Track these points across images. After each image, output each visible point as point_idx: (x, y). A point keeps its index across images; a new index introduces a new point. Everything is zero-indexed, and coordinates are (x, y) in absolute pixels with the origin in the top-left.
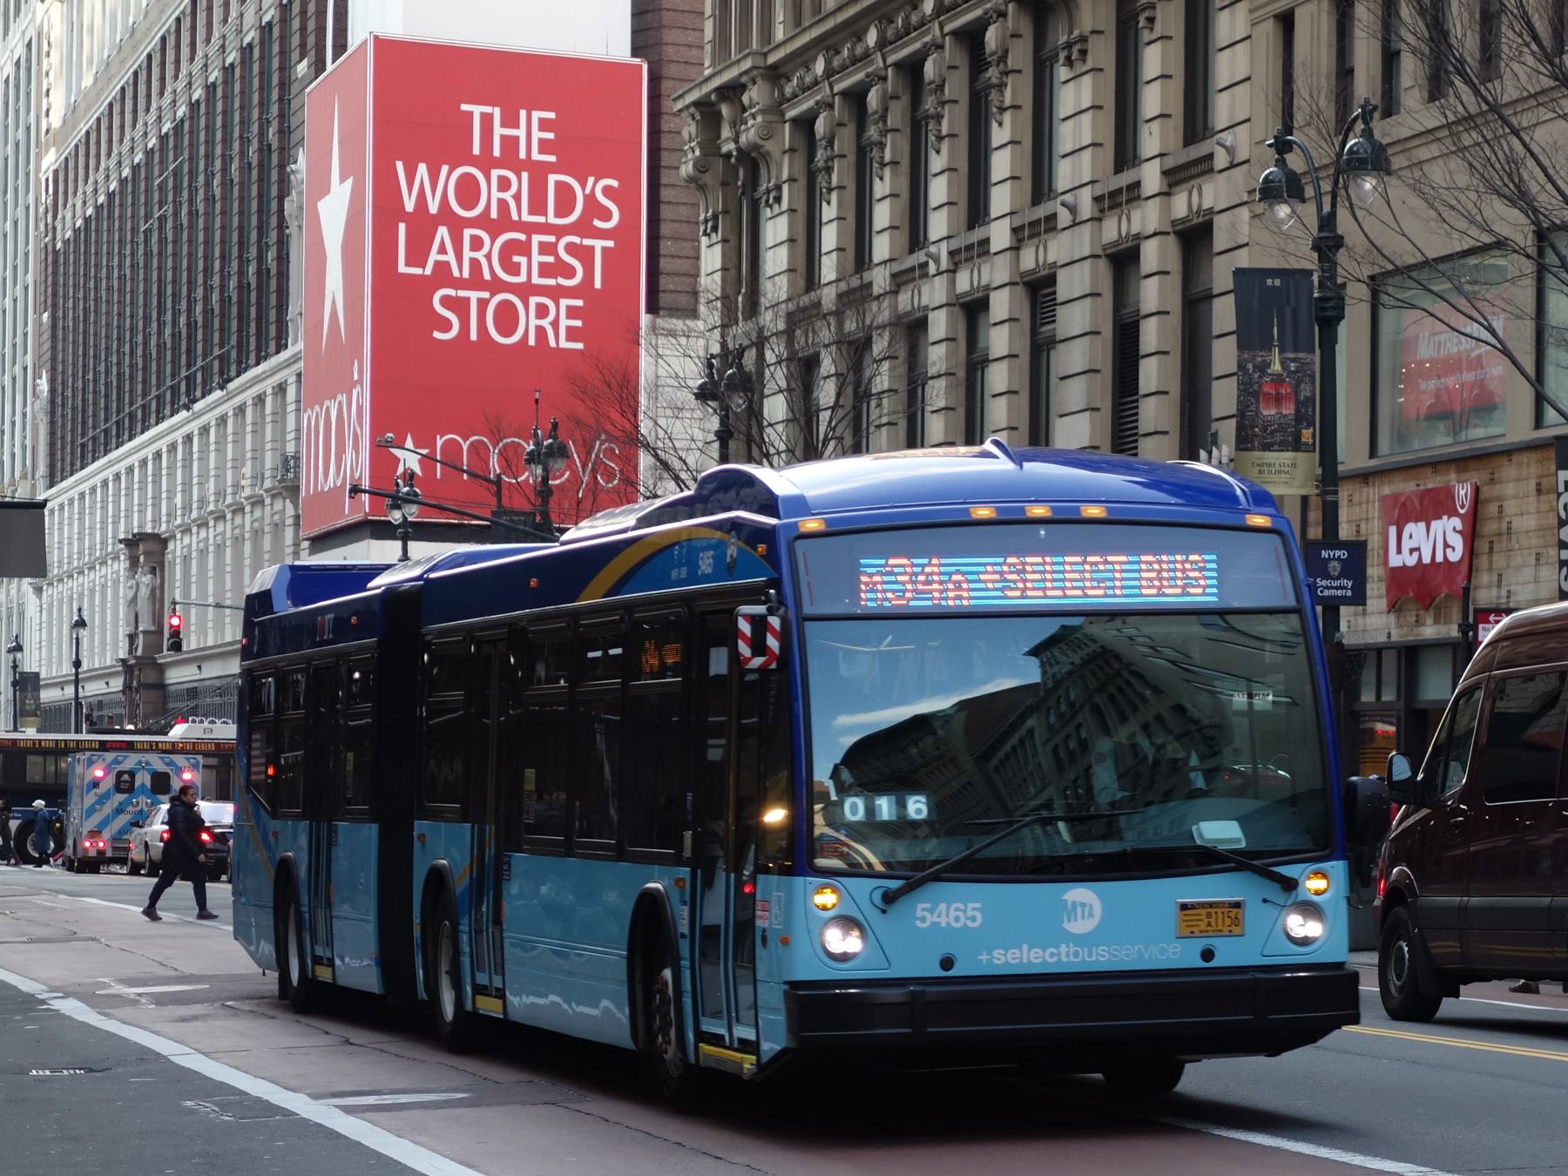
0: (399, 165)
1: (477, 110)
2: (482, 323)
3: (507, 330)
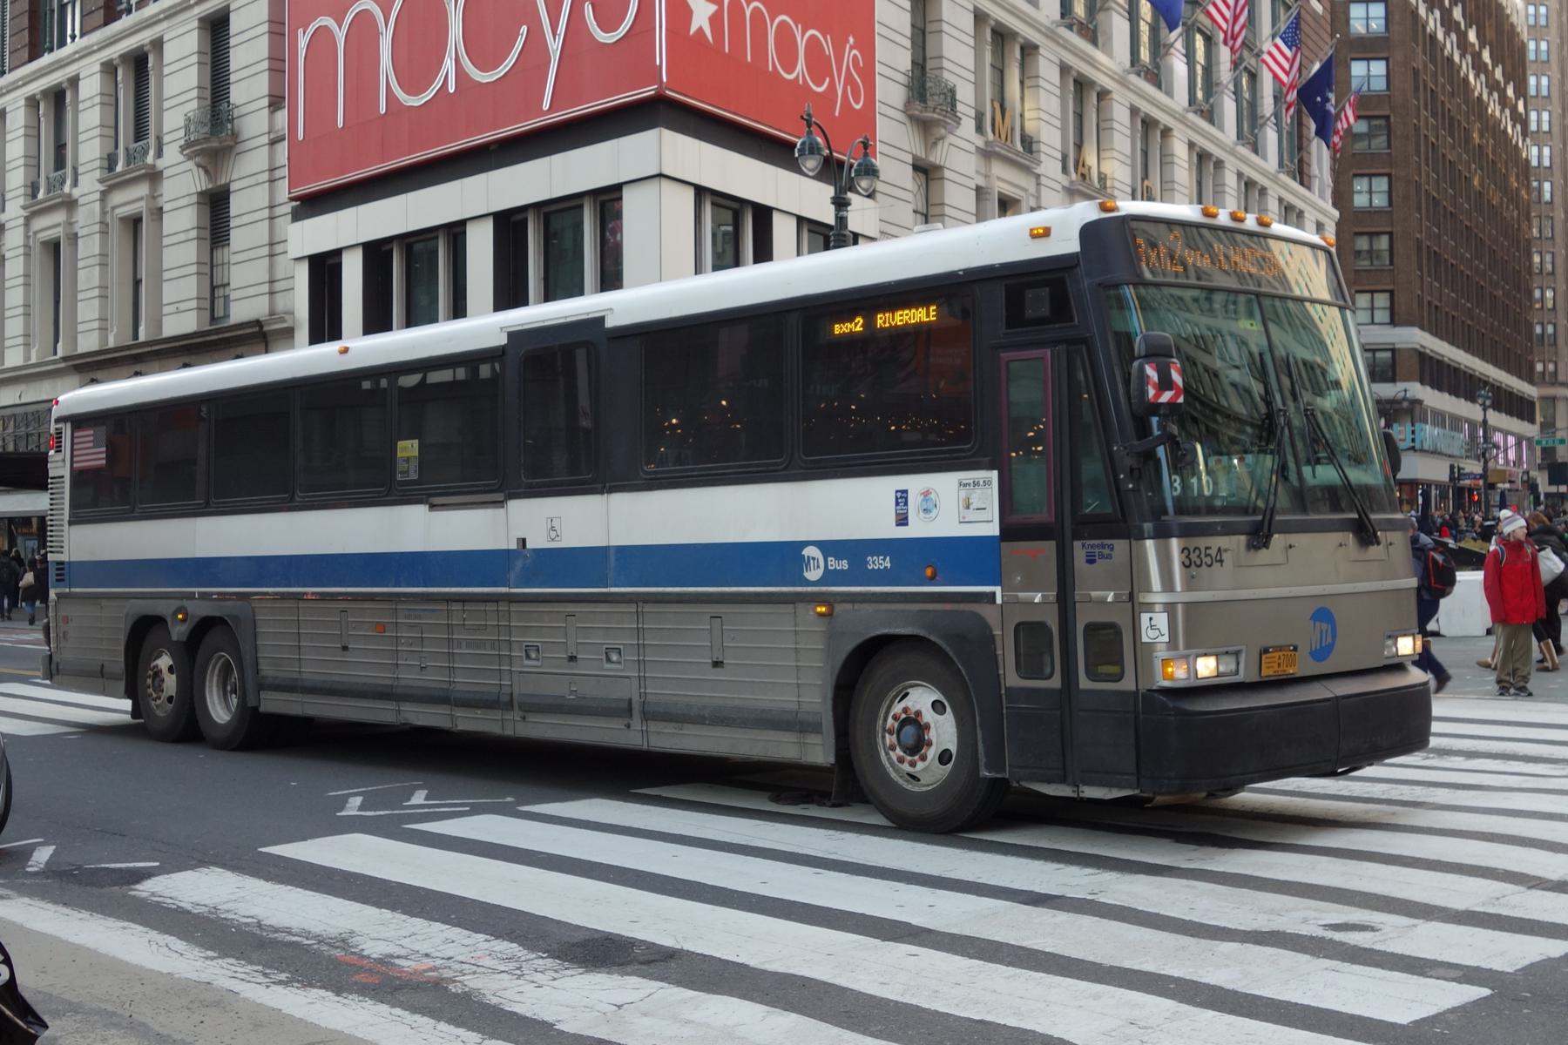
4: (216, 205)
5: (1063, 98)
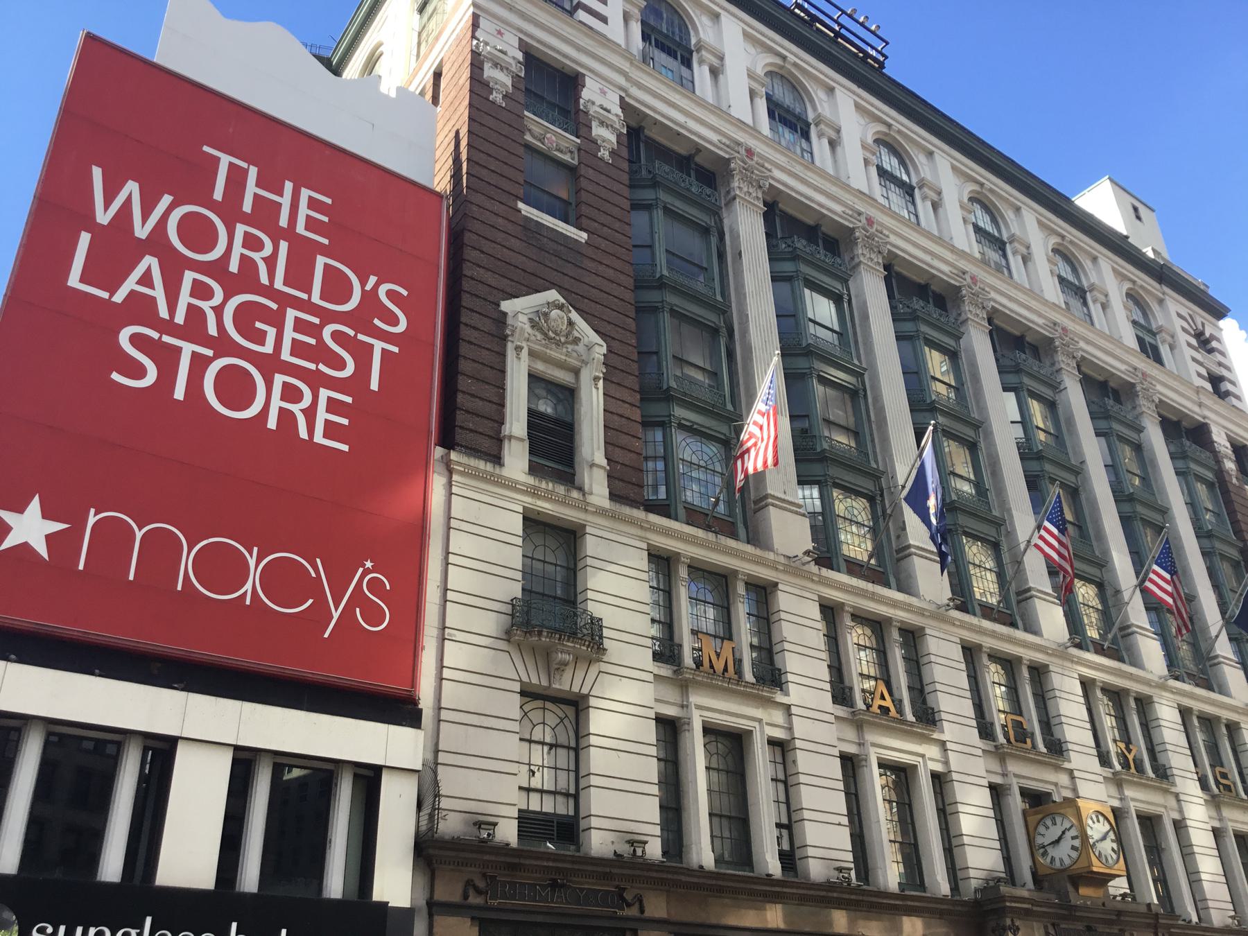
0: (97, 173)
1: (225, 160)
2: (196, 375)
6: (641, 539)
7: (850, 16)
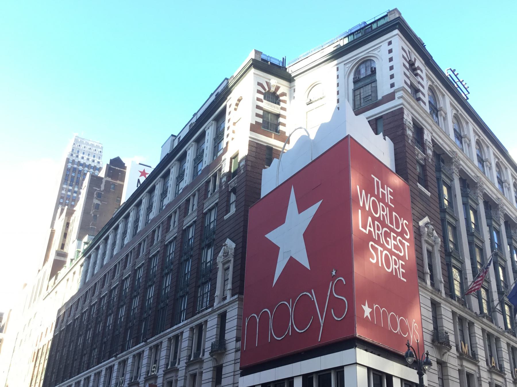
1: (376, 179)
3: (389, 268)
4: (218, 371)
5: (484, 340)
6: (451, 308)
7: (461, 82)
